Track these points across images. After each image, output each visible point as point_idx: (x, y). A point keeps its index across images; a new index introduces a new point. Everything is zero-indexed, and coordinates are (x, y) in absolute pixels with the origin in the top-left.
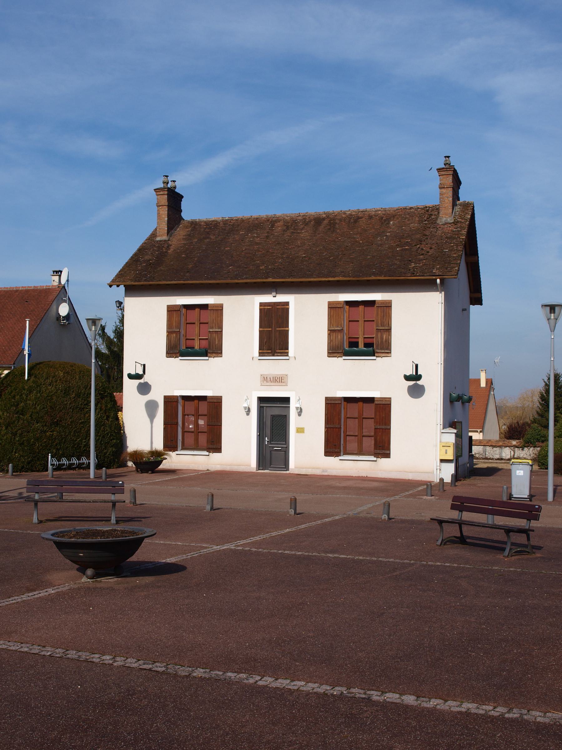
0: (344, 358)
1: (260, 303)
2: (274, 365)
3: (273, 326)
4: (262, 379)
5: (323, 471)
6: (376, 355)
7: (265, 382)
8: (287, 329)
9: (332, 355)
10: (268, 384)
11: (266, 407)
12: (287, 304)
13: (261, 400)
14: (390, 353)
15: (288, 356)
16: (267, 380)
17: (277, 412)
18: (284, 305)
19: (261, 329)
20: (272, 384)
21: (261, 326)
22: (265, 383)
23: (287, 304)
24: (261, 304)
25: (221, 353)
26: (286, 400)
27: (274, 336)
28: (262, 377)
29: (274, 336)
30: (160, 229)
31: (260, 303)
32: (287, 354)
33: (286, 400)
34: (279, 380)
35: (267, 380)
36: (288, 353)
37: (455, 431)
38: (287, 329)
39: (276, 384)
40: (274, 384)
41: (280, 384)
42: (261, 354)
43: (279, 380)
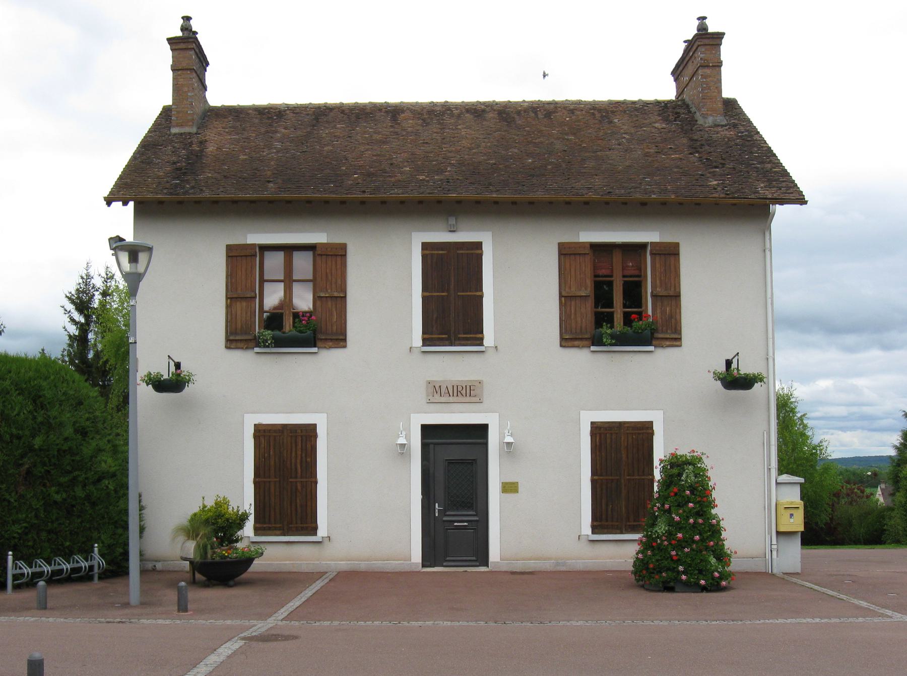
0: (593, 348)
1: (423, 244)
2: (453, 365)
3: (452, 286)
4: (431, 390)
5: (558, 564)
6: (654, 342)
7: (437, 396)
8: (478, 293)
9: (570, 344)
10: (443, 399)
11: (435, 444)
12: (479, 245)
13: (427, 430)
14: (680, 339)
15: (481, 344)
16: (441, 392)
17: (457, 452)
18: (461, 249)
19: (427, 294)
20: (451, 399)
21: (425, 288)
22: (437, 398)
23: (479, 245)
24: (425, 246)
25: (345, 340)
26: (482, 430)
27: (453, 310)
28: (431, 385)
29: (453, 310)
30: (178, 112)
31: (423, 244)
32: (480, 342)
33: (482, 430)
34: (466, 392)
35: (441, 392)
36: (482, 339)
37: (802, 480)
38: (478, 293)
39: (460, 399)
40: (455, 399)
41: (468, 399)
42: (426, 342)
43: (466, 392)
